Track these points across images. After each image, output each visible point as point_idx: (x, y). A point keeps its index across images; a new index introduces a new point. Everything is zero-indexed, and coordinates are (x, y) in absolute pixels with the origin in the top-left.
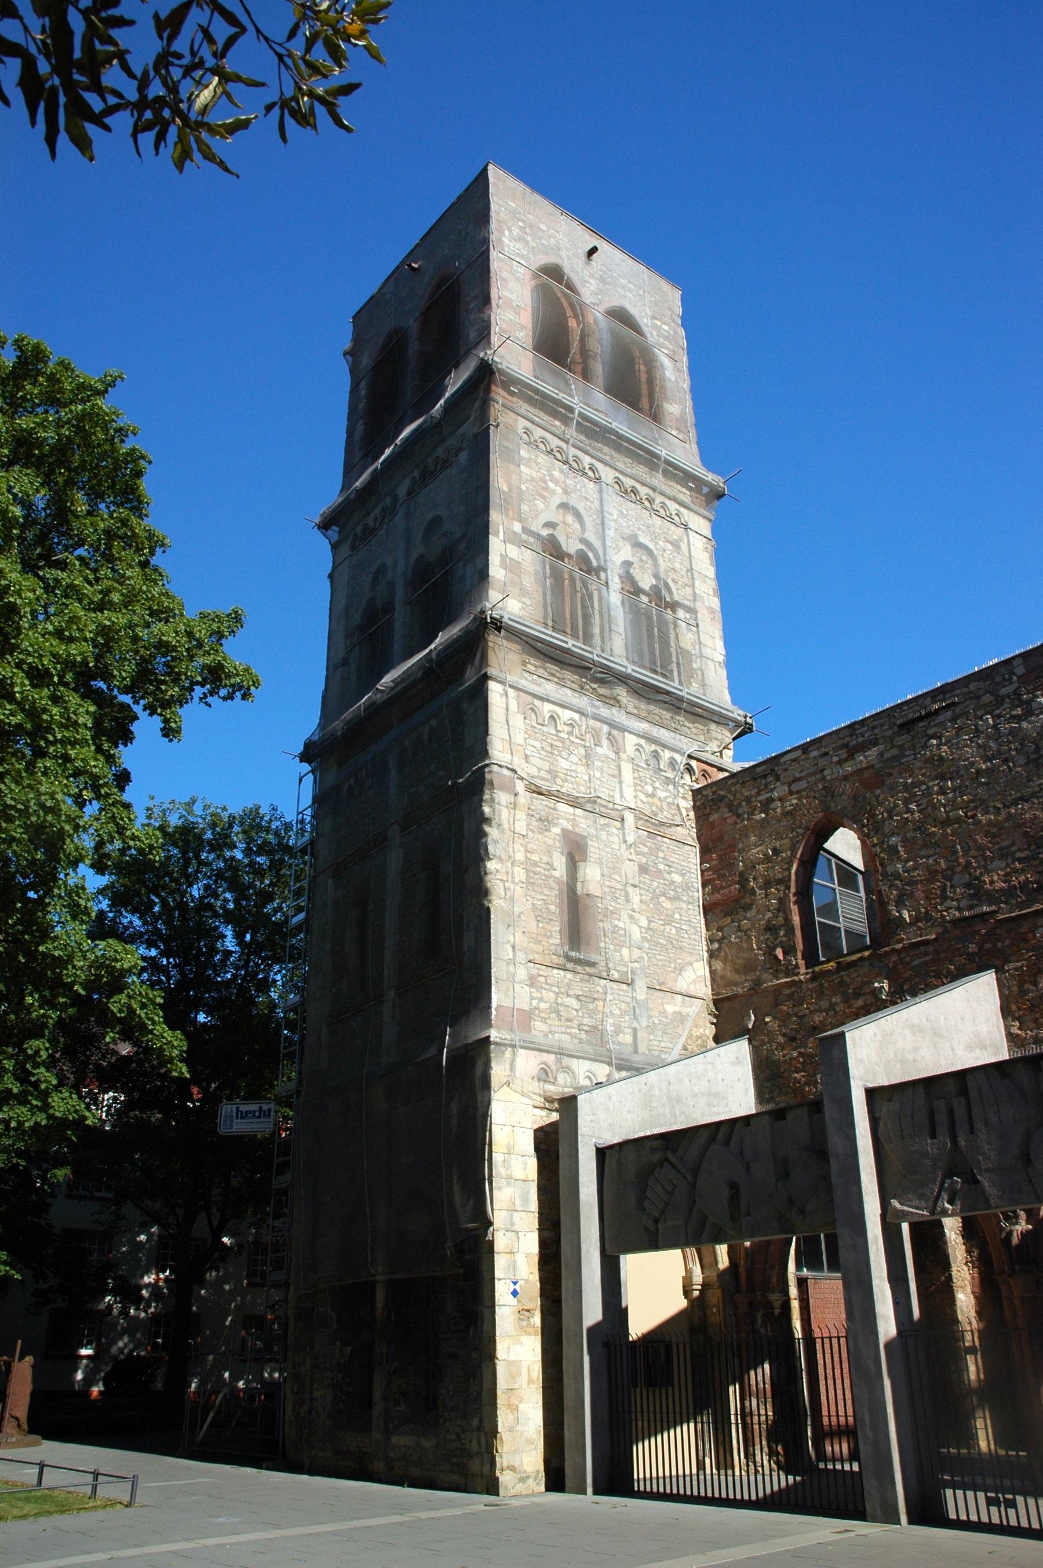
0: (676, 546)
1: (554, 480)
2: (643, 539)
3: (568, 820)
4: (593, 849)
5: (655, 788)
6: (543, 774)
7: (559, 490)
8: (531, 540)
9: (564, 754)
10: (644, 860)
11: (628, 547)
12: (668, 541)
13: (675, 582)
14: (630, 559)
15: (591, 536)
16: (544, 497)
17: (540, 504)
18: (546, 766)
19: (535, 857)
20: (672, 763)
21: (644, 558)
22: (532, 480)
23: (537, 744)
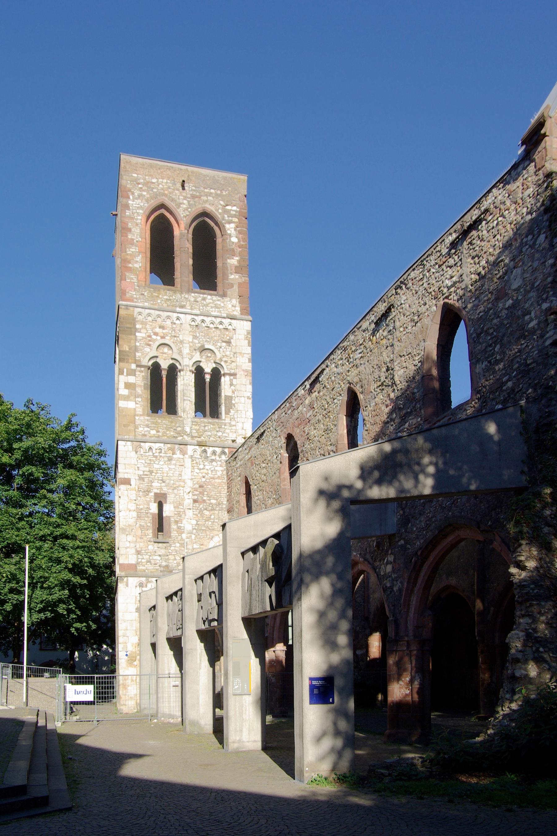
0: (229, 343)
1: (156, 334)
2: (207, 346)
3: (158, 489)
4: (170, 498)
5: (204, 465)
6: (145, 473)
7: (159, 338)
8: (143, 369)
9: (157, 462)
10: (196, 497)
11: (198, 353)
12: (223, 342)
13: (226, 362)
14: (199, 359)
15: (175, 356)
16: (149, 345)
17: (147, 349)
18: (147, 469)
19: (141, 507)
20: (214, 453)
21: (209, 355)
22: (143, 338)
23: (143, 461)
